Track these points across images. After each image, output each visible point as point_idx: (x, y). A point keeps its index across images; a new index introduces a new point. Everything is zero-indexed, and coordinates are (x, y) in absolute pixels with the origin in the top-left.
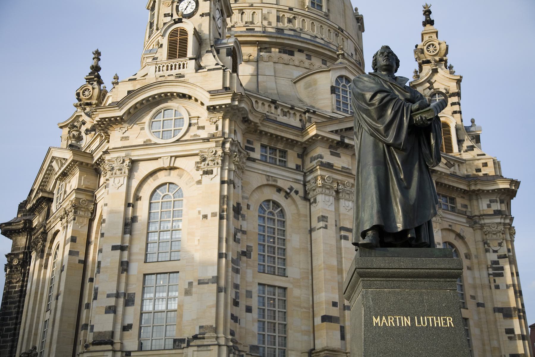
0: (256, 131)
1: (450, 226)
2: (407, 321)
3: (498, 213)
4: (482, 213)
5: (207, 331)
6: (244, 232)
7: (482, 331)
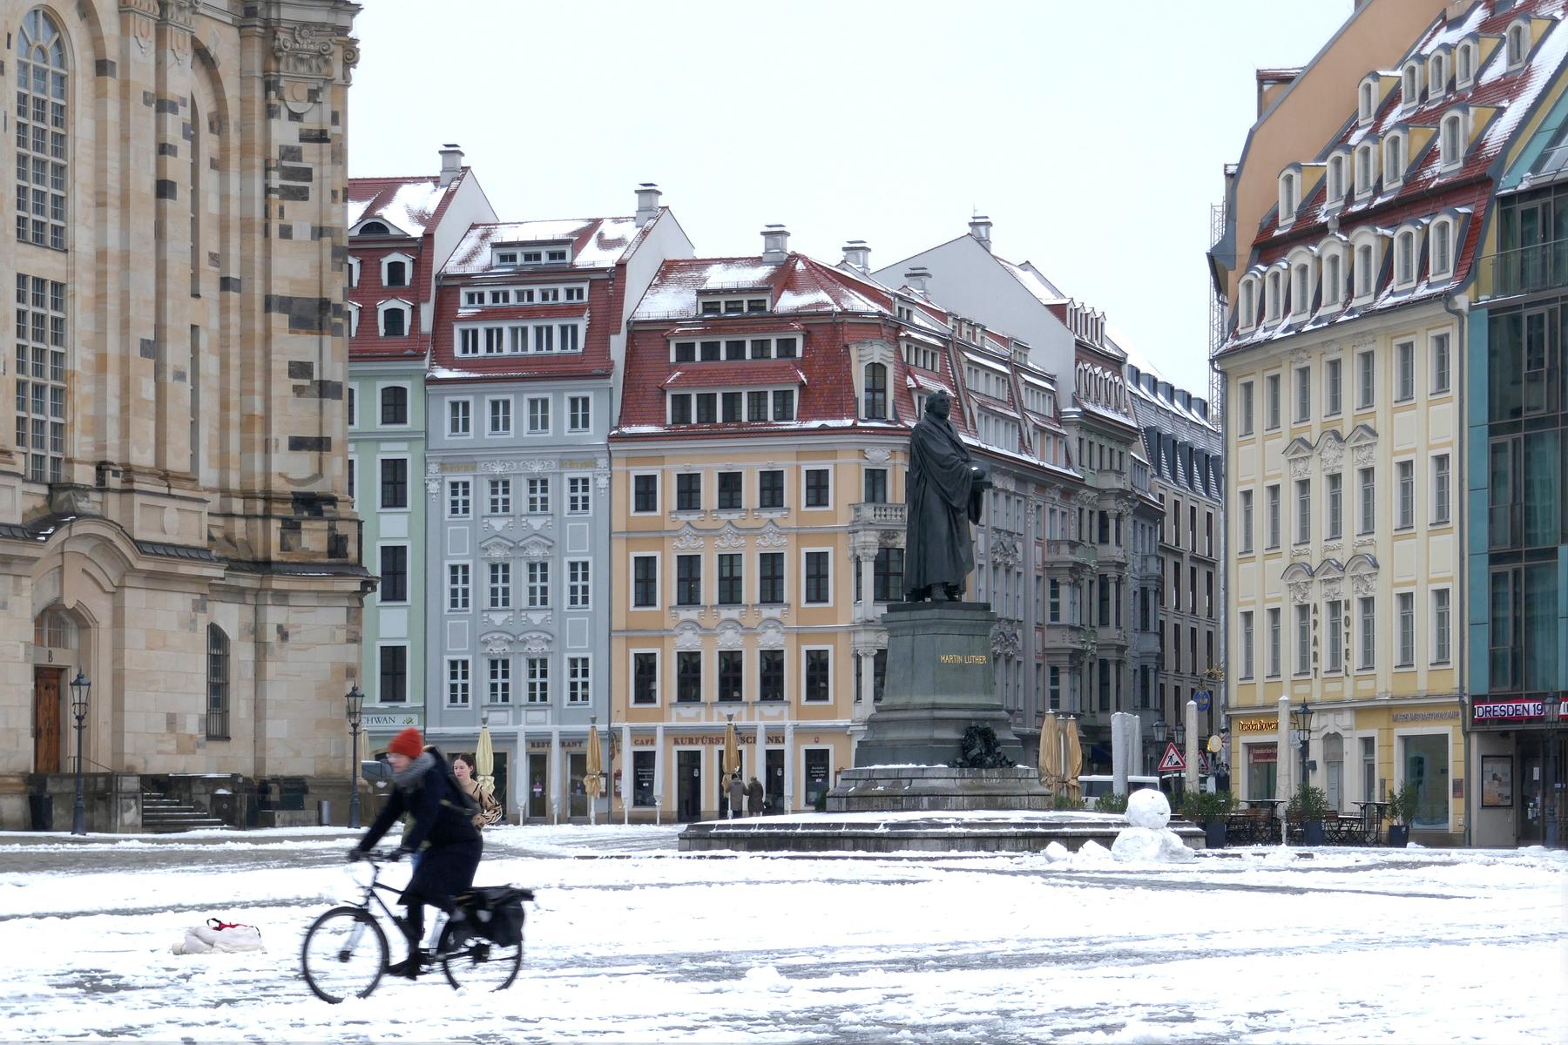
2: (960, 659)
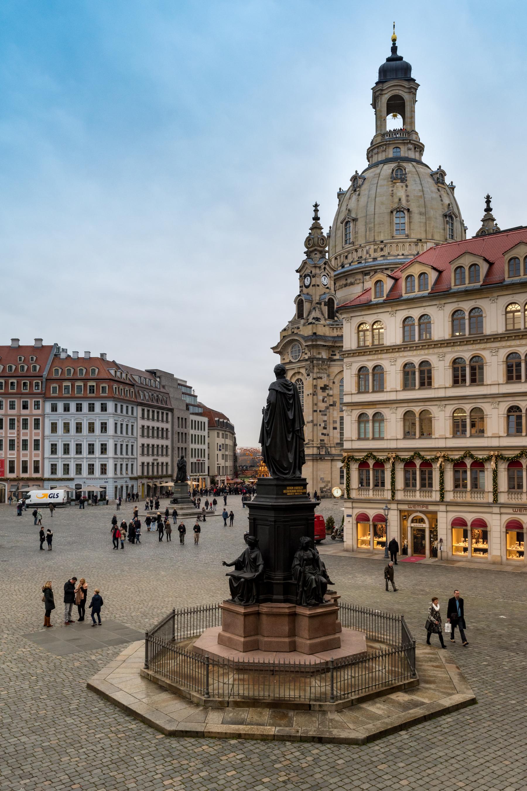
6: (331, 396)
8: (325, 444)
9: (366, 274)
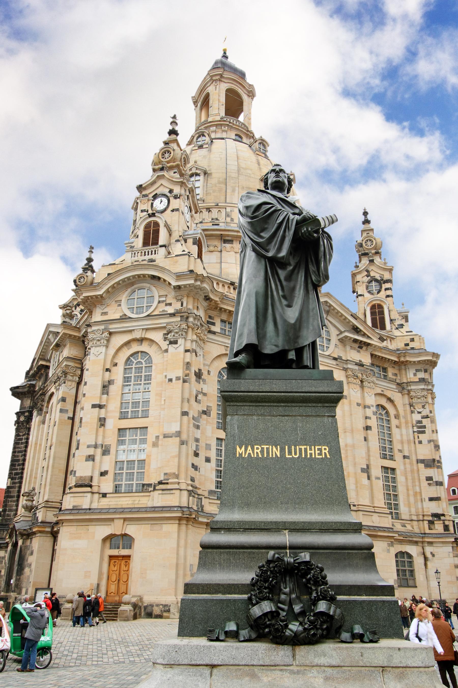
0: (216, 308)
1: (382, 391)
2: (276, 451)
3: (422, 380)
4: (409, 381)
5: (169, 477)
6: (205, 394)
7: (406, 479)
8: (196, 488)
9: (226, 241)
